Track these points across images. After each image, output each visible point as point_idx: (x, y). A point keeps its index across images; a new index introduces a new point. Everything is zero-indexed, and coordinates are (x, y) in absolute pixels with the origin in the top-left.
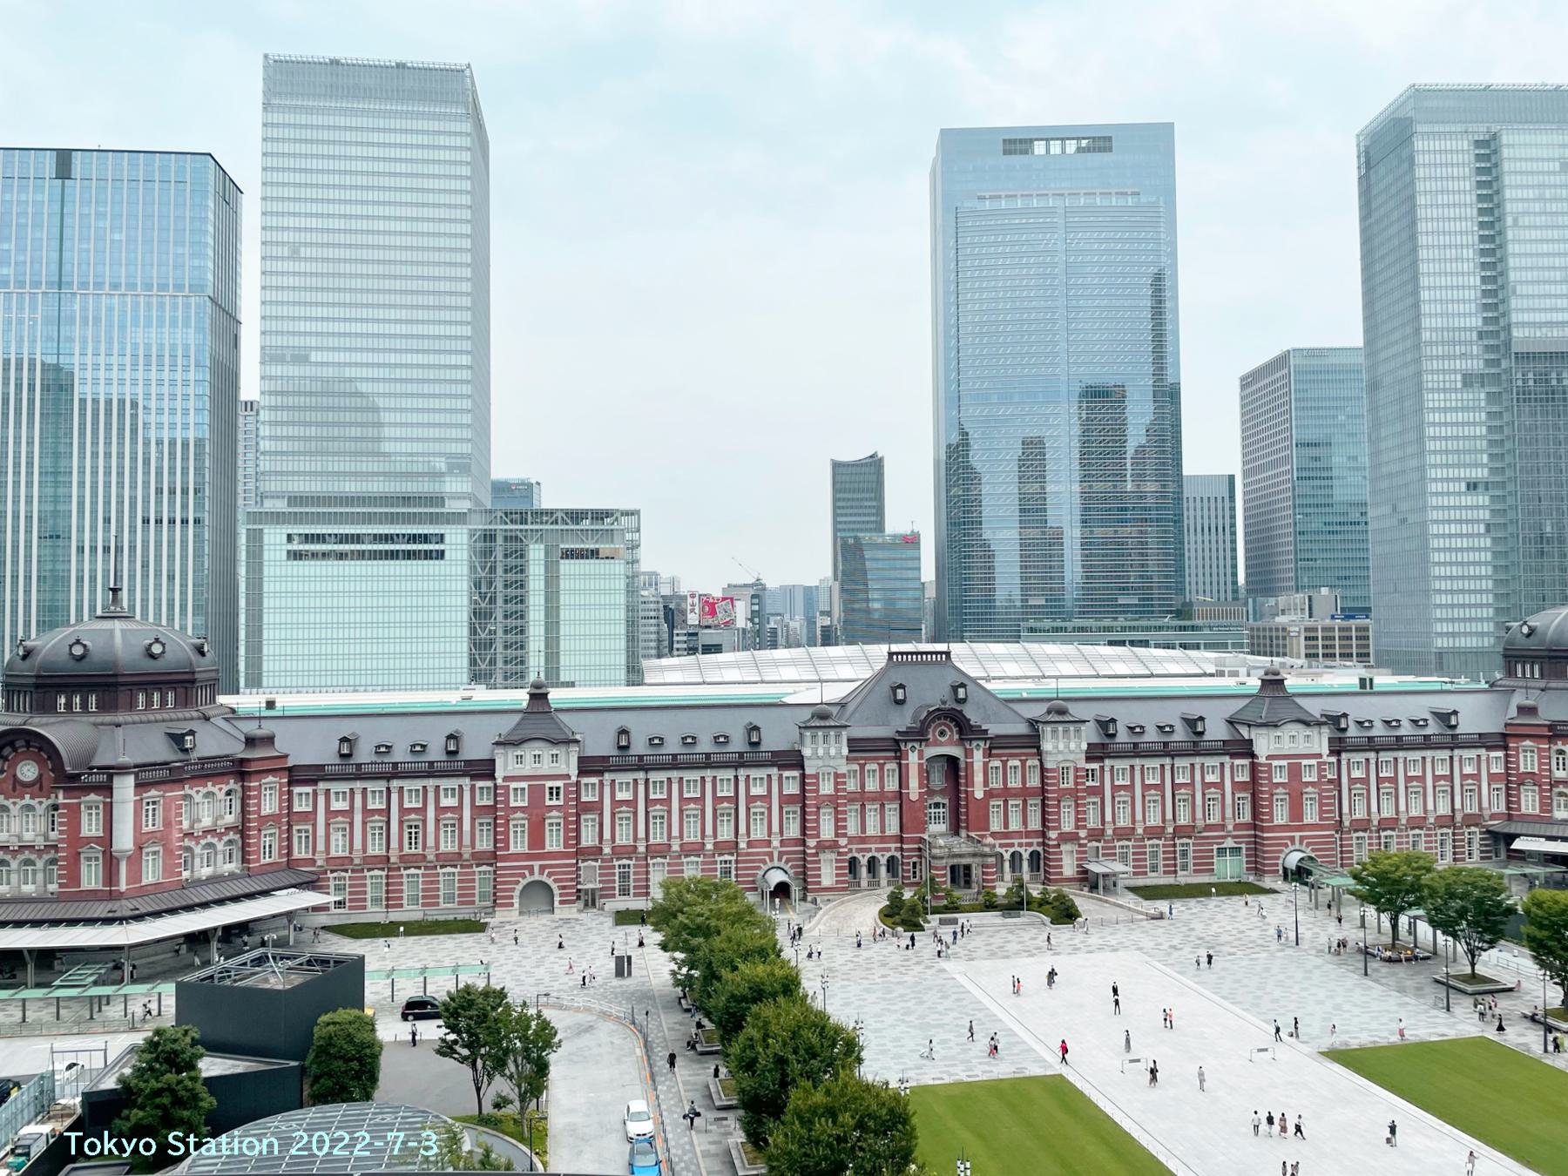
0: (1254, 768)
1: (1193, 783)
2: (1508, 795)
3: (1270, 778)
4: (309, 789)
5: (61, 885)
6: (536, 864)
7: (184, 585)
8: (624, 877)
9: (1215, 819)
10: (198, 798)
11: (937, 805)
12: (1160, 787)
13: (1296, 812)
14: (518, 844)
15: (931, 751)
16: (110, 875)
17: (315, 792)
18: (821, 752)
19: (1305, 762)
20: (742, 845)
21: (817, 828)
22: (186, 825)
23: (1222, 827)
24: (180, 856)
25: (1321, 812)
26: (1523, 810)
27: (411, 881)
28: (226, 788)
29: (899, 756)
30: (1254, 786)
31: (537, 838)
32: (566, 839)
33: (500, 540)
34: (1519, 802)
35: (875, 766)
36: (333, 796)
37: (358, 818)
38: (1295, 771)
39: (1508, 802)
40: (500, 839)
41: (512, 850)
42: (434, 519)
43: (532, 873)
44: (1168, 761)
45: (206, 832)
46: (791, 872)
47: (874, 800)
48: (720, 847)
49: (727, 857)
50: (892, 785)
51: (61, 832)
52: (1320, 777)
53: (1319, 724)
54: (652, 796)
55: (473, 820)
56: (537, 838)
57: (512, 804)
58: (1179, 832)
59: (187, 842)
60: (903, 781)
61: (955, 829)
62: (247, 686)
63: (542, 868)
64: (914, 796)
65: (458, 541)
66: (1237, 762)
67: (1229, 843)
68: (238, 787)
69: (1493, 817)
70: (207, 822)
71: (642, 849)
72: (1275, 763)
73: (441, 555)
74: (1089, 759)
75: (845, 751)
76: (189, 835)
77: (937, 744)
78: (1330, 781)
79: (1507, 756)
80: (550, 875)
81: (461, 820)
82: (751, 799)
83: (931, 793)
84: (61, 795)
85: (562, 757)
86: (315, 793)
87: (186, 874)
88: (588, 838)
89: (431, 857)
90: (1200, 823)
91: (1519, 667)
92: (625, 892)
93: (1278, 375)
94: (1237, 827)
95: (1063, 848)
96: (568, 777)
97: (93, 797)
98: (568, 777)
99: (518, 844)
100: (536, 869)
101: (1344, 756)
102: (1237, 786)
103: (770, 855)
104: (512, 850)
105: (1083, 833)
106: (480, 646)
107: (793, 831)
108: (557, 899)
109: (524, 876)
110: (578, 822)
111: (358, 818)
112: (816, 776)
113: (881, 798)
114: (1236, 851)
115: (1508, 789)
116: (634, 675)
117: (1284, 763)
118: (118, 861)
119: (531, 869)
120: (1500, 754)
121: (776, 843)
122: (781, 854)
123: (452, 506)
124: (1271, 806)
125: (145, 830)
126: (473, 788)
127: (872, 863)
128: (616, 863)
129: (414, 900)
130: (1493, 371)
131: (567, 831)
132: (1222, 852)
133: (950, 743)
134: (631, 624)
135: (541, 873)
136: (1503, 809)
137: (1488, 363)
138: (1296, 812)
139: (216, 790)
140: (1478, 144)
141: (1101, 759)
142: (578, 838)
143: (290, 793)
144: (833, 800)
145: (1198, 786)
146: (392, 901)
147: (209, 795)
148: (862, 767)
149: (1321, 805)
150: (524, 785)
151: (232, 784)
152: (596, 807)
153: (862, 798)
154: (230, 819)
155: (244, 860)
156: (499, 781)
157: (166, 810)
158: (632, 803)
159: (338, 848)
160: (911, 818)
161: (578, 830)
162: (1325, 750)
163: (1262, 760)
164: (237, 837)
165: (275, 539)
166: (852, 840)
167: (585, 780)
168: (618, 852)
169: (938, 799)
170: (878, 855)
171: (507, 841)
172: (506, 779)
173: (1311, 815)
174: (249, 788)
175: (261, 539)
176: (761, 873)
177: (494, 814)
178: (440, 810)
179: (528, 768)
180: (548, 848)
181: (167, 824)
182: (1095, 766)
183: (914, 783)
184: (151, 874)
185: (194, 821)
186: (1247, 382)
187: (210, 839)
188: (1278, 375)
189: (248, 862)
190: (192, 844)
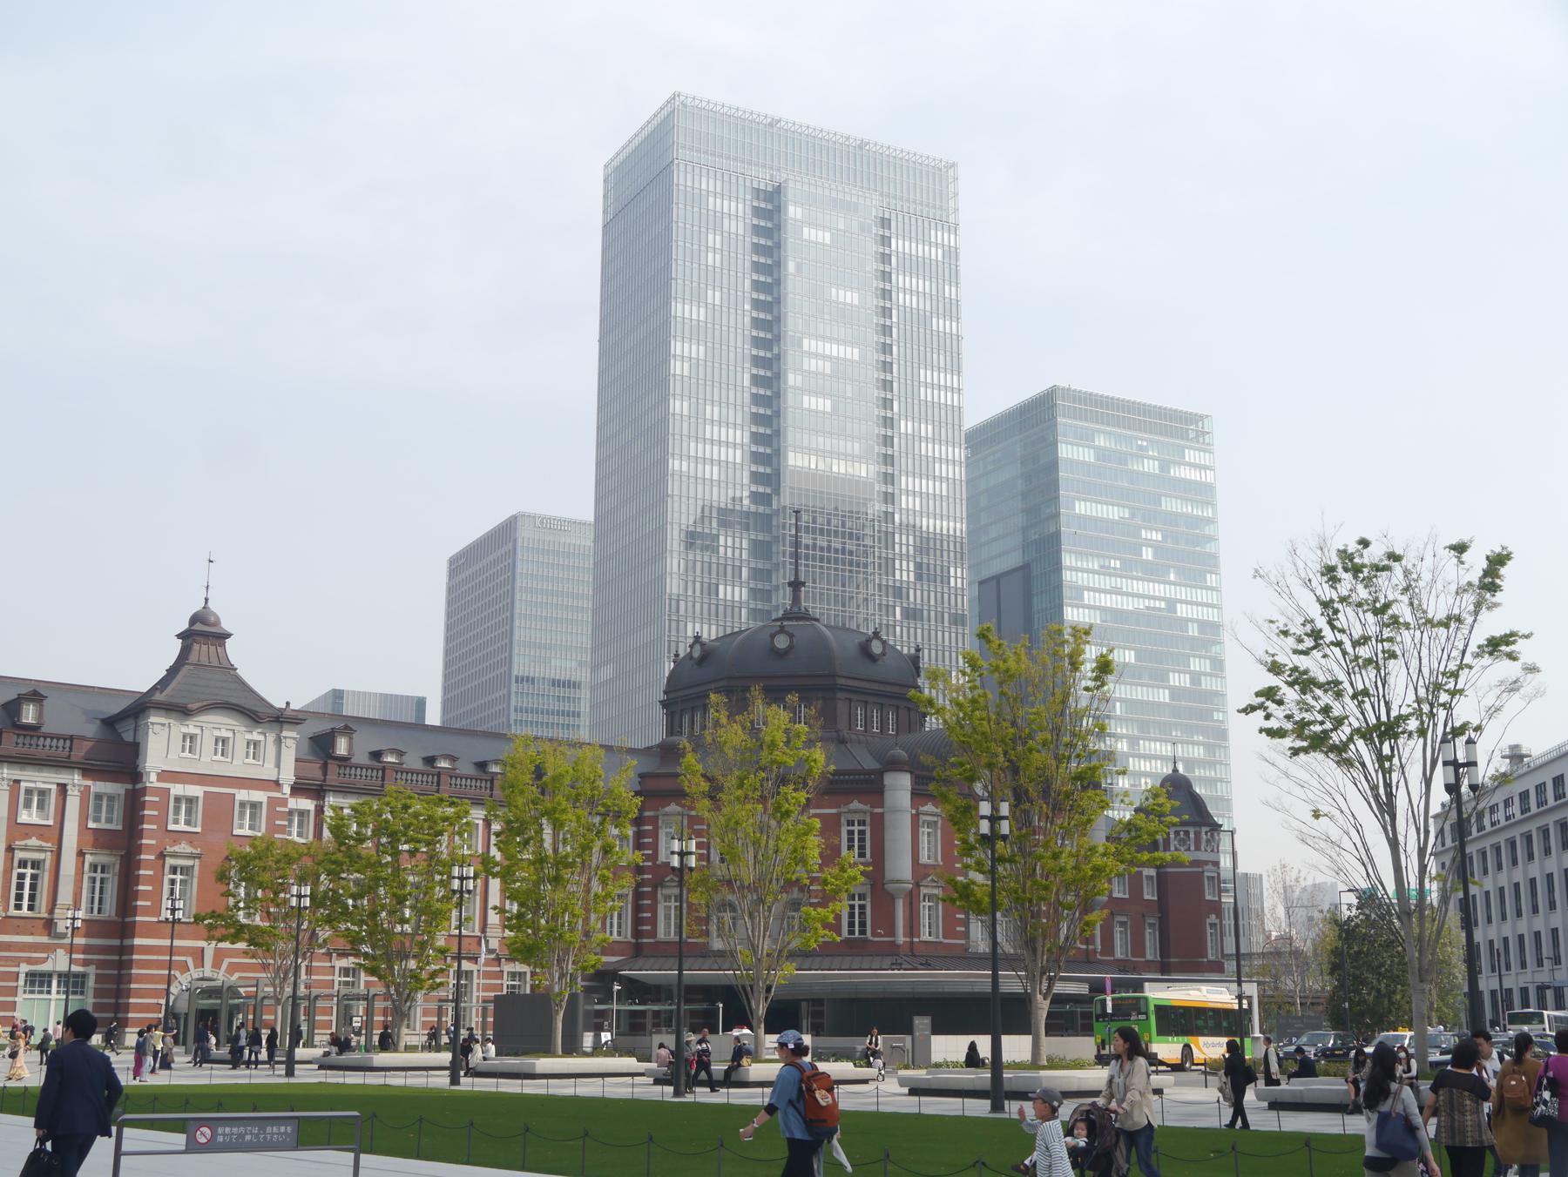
2: (637, 909)
3: (162, 821)
19: (242, 795)
23: (49, 925)
26: (661, 935)
34: (653, 921)
39: (637, 921)
67: (60, 962)
72: (177, 789)
91: (687, 719)
93: (499, 553)
101: (331, 800)
130: (761, 509)
136: (628, 935)
137: (755, 497)
162: (288, 776)
163: (152, 780)
186: (458, 565)
188: (499, 553)
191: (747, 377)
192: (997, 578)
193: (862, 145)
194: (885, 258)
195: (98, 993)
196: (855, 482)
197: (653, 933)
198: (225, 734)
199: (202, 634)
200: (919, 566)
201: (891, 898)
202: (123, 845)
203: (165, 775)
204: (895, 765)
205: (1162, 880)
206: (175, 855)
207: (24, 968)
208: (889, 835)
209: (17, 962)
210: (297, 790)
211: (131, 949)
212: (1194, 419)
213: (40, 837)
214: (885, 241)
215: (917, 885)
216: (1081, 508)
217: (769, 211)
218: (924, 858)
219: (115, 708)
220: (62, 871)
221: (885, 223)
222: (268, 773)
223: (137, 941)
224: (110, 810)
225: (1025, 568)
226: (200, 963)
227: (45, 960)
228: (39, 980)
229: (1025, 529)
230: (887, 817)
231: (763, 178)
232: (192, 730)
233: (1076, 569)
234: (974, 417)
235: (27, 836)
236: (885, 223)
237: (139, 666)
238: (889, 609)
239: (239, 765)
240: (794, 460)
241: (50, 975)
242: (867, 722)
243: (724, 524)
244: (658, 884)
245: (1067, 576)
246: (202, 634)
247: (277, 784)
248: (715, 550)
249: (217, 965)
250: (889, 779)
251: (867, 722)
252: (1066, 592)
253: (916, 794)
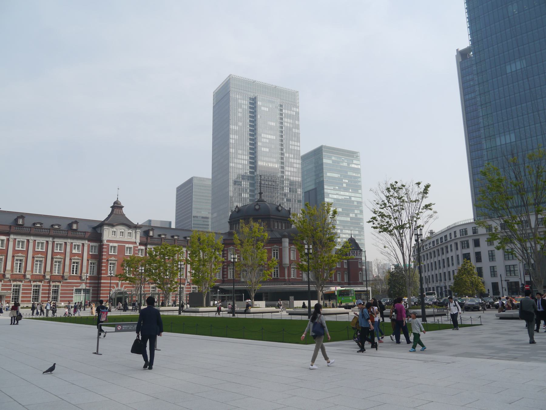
2: (223, 272)
3: (108, 252)
19: (127, 245)
23: (80, 278)
26: (229, 278)
34: (227, 275)
39: (223, 275)
44: (51, 239)
67: (83, 286)
72: (111, 244)
91: (234, 226)
137: (251, 172)
162: (138, 241)
163: (105, 242)
186: (179, 189)
191: (248, 143)
192: (309, 191)
193: (276, 87)
194: (281, 114)
195: (93, 294)
196: (275, 169)
197: (227, 277)
198: (122, 231)
199: (117, 207)
200: (290, 189)
201: (284, 268)
202: (98, 258)
203: (108, 241)
204: (285, 236)
205: (348, 263)
206: (111, 260)
207: (75, 288)
208: (283, 253)
209: (73, 286)
210: (140, 244)
211: (101, 283)
212: (356, 153)
213: (78, 256)
214: (281, 110)
215: (290, 265)
216: (329, 174)
217: (253, 103)
218: (292, 259)
219: (96, 225)
220: (83, 265)
221: (281, 106)
223: (102, 281)
224: (95, 249)
225: (315, 189)
226: (117, 286)
227: (79, 286)
228: (78, 291)
229: (315, 180)
230: (283, 249)
231: (252, 95)
232: (115, 230)
233: (328, 189)
234: (303, 152)
235: (75, 256)
236: (281, 106)
237: (101, 214)
238: (283, 199)
239: (126, 238)
240: (260, 163)
241: (81, 290)
242: (278, 227)
243: (243, 179)
244: (228, 266)
245: (325, 191)
246: (117, 207)
247: (135, 243)
248: (241, 185)
249: (122, 286)
250: (283, 240)
251: (278, 227)
252: (325, 195)
253: (290, 244)
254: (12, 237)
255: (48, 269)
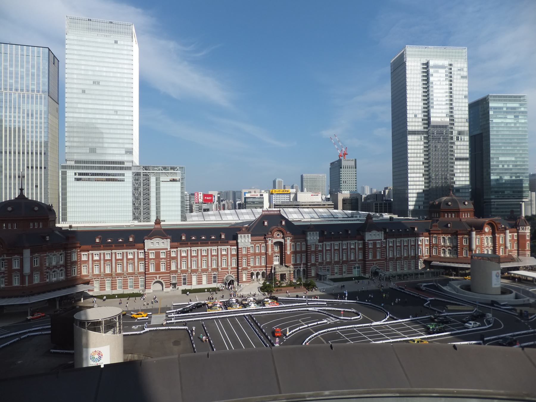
0: (364, 244)
1: (347, 248)
2: (430, 250)
3: (368, 246)
4: (86, 253)
5: (6, 285)
6: (158, 276)
7: (41, 189)
8: (184, 279)
9: (352, 259)
10: (51, 256)
11: (276, 256)
12: (339, 250)
13: (375, 256)
14: (152, 269)
15: (275, 240)
16: (22, 281)
17: (88, 254)
18: (243, 241)
19: (377, 242)
20: (220, 269)
21: (242, 264)
22: (47, 265)
24: (45, 275)
25: (381, 256)
27: (119, 281)
28: (60, 253)
29: (266, 242)
30: (364, 249)
31: (158, 268)
32: (167, 268)
33: (142, 175)
35: (259, 245)
36: (94, 255)
37: (102, 262)
38: (375, 244)
39: (430, 252)
40: (146, 268)
41: (150, 271)
42: (121, 168)
43: (156, 278)
45: (54, 267)
46: (234, 277)
47: (258, 255)
48: (213, 270)
49: (215, 273)
50: (263, 251)
51: (6, 268)
52: (381, 246)
53: (381, 231)
54: (193, 255)
55: (138, 262)
56: (158, 268)
57: (150, 257)
58: (344, 262)
59: (48, 270)
60: (267, 250)
61: (281, 263)
62: (62, 221)
63: (160, 277)
64: (270, 254)
65: (129, 175)
66: (359, 242)
67: (357, 265)
68: (64, 252)
69: (426, 256)
70: (54, 263)
71: (190, 271)
72: (370, 242)
73: (123, 181)
74: (319, 242)
75: (250, 241)
76: (48, 268)
77: (277, 238)
78: (384, 247)
79: (430, 239)
80: (162, 279)
81: (134, 262)
82: (222, 255)
83: (275, 253)
84: (5, 256)
85: (165, 243)
86: (88, 254)
87: (48, 280)
88: (173, 268)
89: (125, 274)
90: (349, 260)
92: (185, 284)
94: (359, 260)
95: (312, 268)
96: (167, 249)
97: (16, 256)
98: (167, 249)
99: (152, 269)
100: (158, 277)
102: (359, 249)
103: (228, 272)
104: (150, 271)
105: (317, 264)
106: (136, 208)
107: (234, 265)
108: (164, 286)
109: (154, 279)
110: (170, 263)
111: (102, 262)
112: (241, 248)
113: (260, 254)
114: (358, 268)
115: (430, 248)
116: (184, 218)
117: (372, 242)
118: (25, 276)
119: (156, 277)
120: (428, 238)
121: (229, 268)
122: (231, 272)
123: (126, 165)
124: (368, 254)
125: (34, 266)
126: (138, 253)
127: (258, 274)
128: (182, 275)
129: (120, 287)
131: (167, 265)
132: (355, 268)
133: (280, 238)
134: (182, 202)
135: (159, 278)
138: (375, 256)
139: (49, 254)
140: (423, 64)
141: (323, 242)
142: (170, 268)
143: (80, 254)
144: (246, 255)
145: (349, 249)
146: (125, 286)
147: (54, 255)
148: (255, 245)
149: (381, 254)
150: (154, 251)
151: (62, 252)
152: (175, 258)
153: (255, 254)
154: (62, 263)
155: (66, 276)
156: (146, 250)
157: (41, 260)
158: (187, 257)
159: (96, 272)
160: (269, 260)
161: (170, 265)
162: (383, 238)
163: (366, 241)
164: (64, 268)
165: (71, 174)
166: (252, 267)
167: (172, 250)
168: (183, 272)
169: (277, 255)
170: (259, 271)
171: (149, 269)
172: (148, 250)
173: (378, 258)
174: (68, 253)
175: (66, 174)
176: (225, 278)
177: (146, 260)
178: (128, 259)
179: (157, 246)
180: (161, 271)
181: (41, 264)
182: (321, 244)
183: (270, 250)
184: (37, 280)
185: (50, 263)
187: (55, 269)
189: (68, 276)
190: (50, 271)
192: (475, 136)
196: (447, 122)
203: (368, 240)
216: (495, 121)
218: (477, 244)
222: (380, 238)
231: (425, 61)
240: (432, 119)
254: (324, 243)
255: (341, 258)
